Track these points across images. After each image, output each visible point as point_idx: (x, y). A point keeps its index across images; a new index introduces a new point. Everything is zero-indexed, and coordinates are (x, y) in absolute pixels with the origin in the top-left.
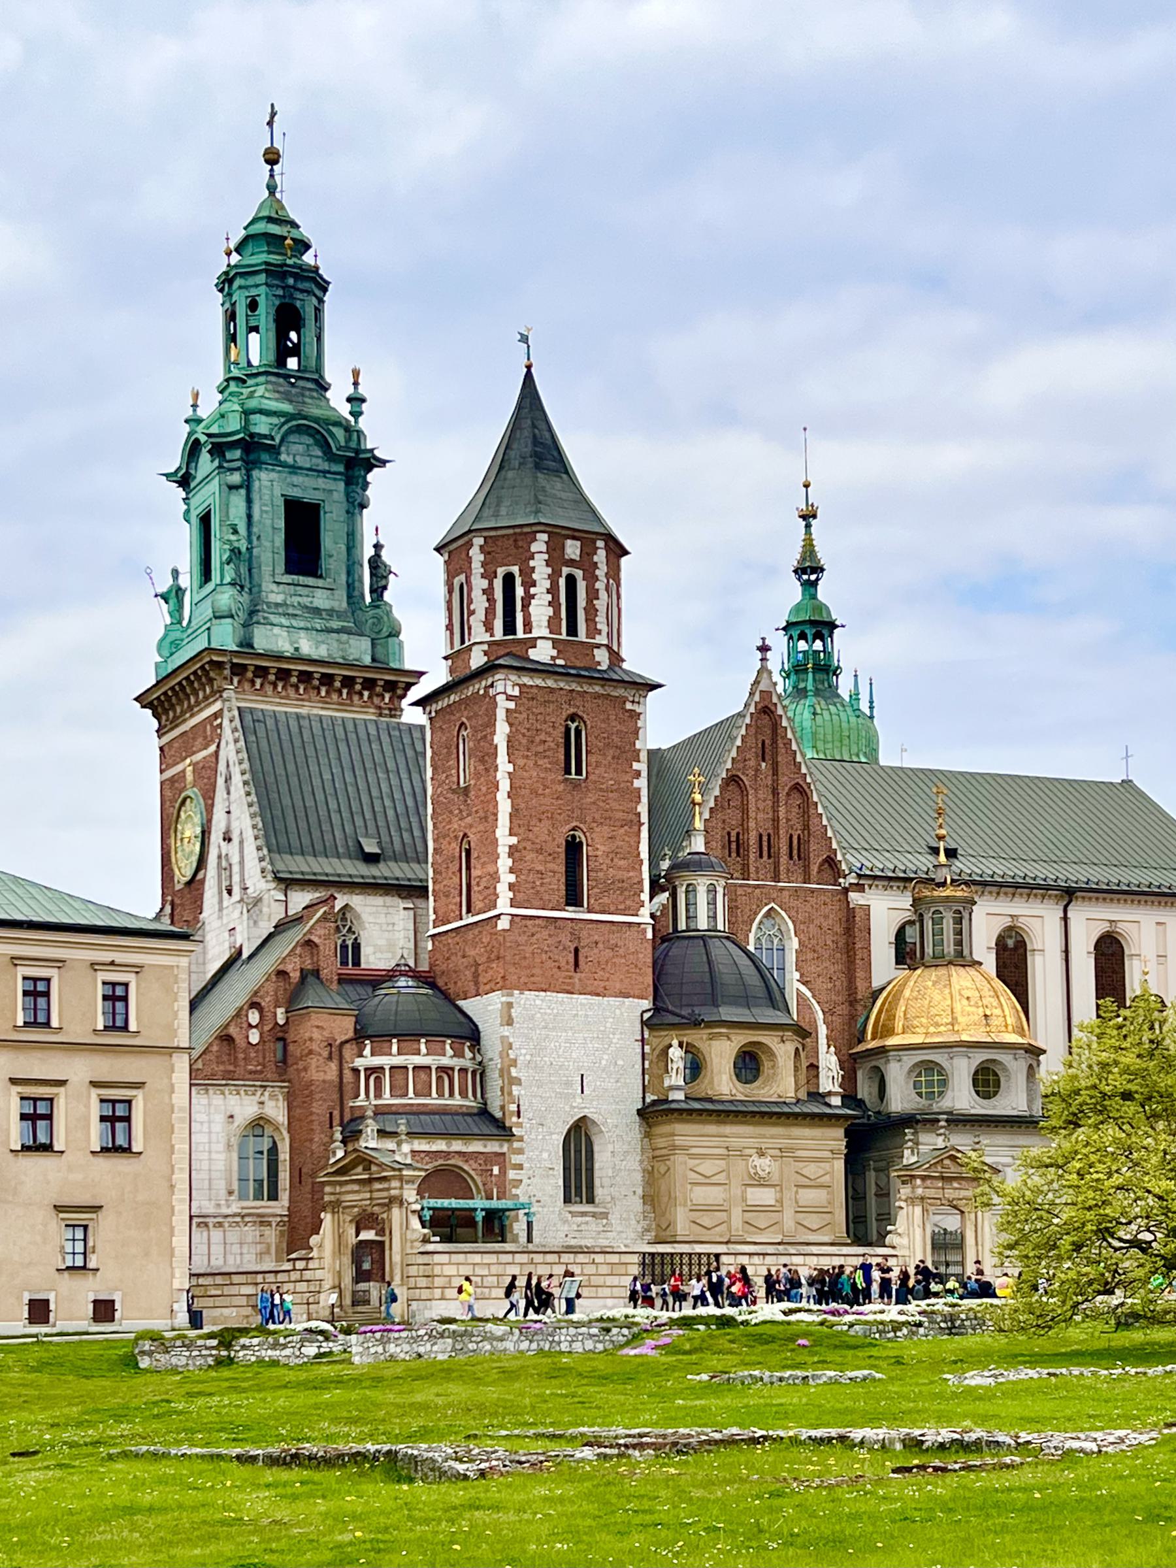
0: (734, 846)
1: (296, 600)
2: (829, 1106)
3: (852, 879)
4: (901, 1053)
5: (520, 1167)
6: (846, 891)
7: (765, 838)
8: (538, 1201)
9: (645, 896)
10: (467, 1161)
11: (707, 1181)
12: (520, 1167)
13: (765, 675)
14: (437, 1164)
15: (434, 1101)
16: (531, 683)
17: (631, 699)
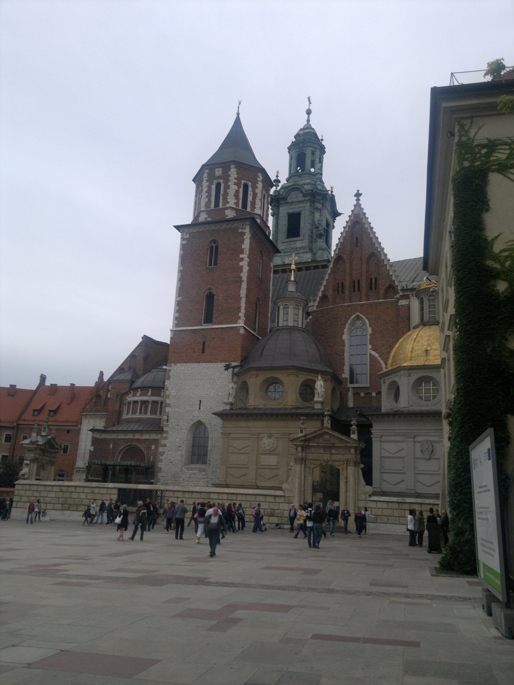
0: (340, 289)
1: (289, 247)
2: (313, 408)
3: (401, 294)
4: (386, 378)
5: (165, 446)
6: (399, 299)
7: (356, 282)
8: (172, 462)
9: (242, 314)
10: (140, 443)
11: (239, 452)
12: (165, 446)
13: (357, 207)
14: (127, 444)
15: (137, 416)
16: (195, 231)
17: (241, 227)
